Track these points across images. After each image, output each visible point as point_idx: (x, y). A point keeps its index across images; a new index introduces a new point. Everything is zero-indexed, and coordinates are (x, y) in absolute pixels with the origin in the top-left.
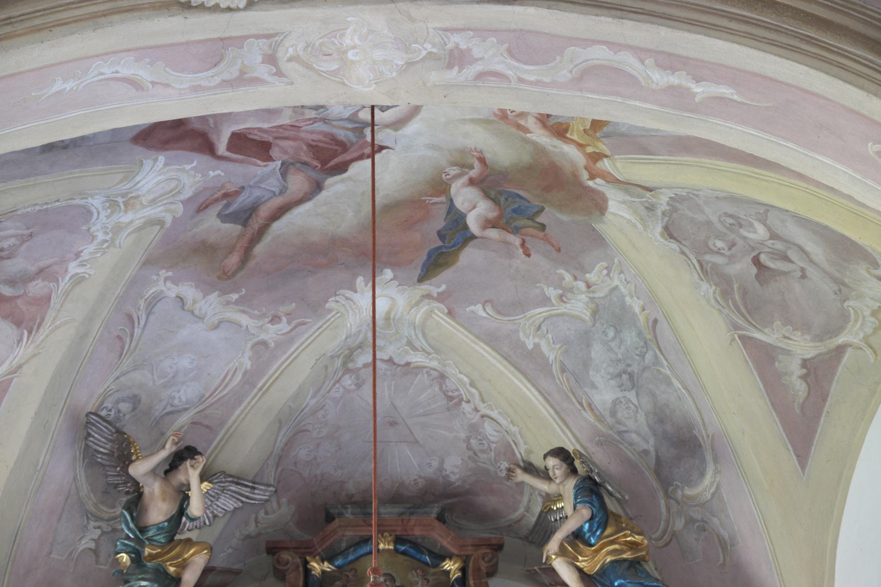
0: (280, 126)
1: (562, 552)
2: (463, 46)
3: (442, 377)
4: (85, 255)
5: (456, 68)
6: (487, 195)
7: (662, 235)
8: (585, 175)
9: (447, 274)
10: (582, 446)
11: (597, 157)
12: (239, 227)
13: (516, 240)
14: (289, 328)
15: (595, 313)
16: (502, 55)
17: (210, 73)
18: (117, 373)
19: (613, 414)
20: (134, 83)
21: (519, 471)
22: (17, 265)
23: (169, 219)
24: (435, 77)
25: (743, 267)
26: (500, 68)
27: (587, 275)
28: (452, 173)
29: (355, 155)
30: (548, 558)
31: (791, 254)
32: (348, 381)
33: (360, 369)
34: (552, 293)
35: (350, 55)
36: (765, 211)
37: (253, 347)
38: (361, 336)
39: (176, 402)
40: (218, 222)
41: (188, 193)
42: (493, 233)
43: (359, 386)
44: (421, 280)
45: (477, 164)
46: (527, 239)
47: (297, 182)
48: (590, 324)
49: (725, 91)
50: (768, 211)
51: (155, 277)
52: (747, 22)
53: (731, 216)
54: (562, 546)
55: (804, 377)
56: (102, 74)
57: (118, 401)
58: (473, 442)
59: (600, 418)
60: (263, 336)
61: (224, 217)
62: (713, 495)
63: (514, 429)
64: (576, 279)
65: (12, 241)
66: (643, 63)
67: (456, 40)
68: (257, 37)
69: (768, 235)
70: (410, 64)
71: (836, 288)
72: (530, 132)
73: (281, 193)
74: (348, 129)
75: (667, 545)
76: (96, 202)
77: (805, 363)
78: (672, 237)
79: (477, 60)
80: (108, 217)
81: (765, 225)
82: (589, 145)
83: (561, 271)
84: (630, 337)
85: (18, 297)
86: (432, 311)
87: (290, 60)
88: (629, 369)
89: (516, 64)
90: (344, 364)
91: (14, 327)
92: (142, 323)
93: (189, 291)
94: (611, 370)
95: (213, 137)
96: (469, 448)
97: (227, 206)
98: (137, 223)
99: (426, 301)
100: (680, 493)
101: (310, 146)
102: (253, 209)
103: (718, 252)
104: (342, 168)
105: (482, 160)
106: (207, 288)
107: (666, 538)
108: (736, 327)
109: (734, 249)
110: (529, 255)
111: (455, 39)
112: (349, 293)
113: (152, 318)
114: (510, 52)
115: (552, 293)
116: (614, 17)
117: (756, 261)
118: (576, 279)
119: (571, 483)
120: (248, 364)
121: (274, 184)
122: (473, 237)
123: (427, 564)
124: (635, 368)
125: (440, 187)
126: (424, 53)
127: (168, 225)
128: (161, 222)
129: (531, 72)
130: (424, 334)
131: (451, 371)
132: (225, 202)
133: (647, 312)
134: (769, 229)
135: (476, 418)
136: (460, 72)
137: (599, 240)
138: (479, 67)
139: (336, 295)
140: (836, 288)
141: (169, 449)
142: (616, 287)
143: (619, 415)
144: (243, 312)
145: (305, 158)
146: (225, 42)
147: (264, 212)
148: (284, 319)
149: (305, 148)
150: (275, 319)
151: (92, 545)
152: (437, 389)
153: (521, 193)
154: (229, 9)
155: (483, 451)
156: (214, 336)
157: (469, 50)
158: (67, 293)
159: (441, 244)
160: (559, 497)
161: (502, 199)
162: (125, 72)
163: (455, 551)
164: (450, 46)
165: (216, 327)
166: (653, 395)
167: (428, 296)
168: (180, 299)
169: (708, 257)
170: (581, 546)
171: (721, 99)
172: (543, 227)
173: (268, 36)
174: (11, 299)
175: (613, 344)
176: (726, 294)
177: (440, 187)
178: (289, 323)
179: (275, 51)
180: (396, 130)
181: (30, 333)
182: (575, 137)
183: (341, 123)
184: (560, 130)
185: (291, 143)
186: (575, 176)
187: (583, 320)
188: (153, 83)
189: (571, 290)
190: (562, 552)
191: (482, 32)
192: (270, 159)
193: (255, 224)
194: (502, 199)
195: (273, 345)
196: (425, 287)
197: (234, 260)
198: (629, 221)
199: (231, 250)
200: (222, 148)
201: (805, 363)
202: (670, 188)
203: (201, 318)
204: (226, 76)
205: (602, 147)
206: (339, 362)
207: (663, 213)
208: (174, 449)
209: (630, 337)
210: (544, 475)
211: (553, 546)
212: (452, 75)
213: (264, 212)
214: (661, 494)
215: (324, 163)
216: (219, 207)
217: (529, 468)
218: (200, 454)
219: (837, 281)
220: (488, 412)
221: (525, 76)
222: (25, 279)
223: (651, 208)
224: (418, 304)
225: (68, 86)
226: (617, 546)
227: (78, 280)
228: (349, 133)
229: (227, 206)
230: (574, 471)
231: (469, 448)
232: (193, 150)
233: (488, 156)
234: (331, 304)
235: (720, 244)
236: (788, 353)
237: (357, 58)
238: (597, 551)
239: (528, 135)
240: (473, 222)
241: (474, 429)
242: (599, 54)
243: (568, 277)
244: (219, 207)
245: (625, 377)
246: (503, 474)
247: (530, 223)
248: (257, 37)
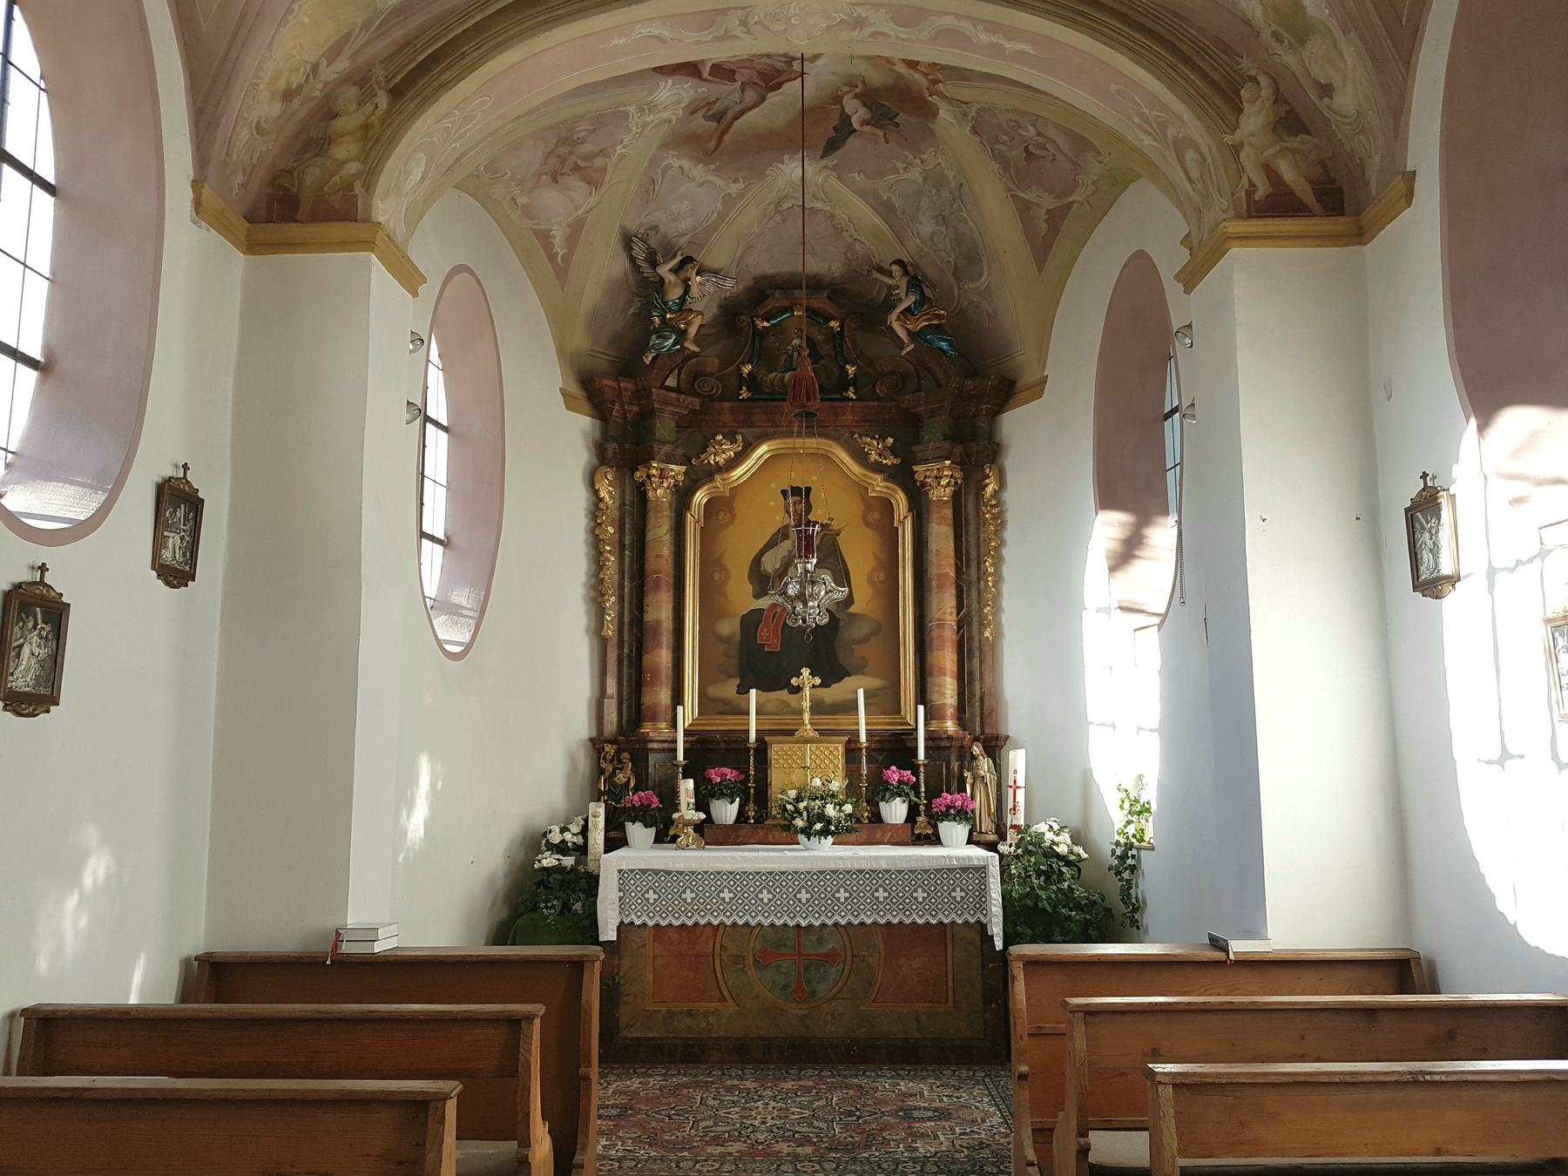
0: (741, 60)
1: (898, 319)
2: (863, 15)
3: (833, 216)
4: (626, 142)
5: (858, 30)
6: (865, 104)
7: (970, 131)
8: (927, 94)
9: (838, 153)
10: (912, 259)
11: (935, 82)
12: (715, 124)
13: (881, 133)
14: (743, 186)
15: (925, 179)
16: (887, 21)
17: (708, 31)
18: (646, 213)
19: (931, 239)
20: (659, 38)
21: (874, 271)
22: (587, 148)
23: (674, 119)
24: (844, 35)
25: (1018, 154)
26: (886, 30)
27: (923, 156)
28: (845, 90)
29: (785, 79)
30: (891, 322)
31: (1048, 146)
32: (778, 218)
33: (784, 211)
34: (900, 166)
36: (1034, 119)
37: (723, 198)
38: (786, 192)
39: (680, 230)
40: (703, 120)
41: (685, 103)
42: (867, 129)
43: (783, 221)
44: (822, 157)
45: (860, 85)
46: (888, 132)
47: (750, 95)
48: (922, 185)
49: (1026, 47)
50: (1037, 119)
51: (666, 155)
53: (1015, 121)
54: (898, 316)
55: (1046, 220)
56: (641, 33)
57: (646, 230)
58: (849, 254)
59: (923, 242)
60: (729, 191)
61: (706, 118)
62: (986, 288)
63: (873, 248)
64: (915, 158)
65: (584, 133)
66: (975, 27)
69: (1035, 133)
70: (829, 27)
71: (1073, 167)
72: (895, 65)
73: (740, 102)
74: (781, 61)
75: (957, 315)
76: (631, 109)
77: (1048, 212)
78: (976, 133)
79: (872, 24)
80: (639, 118)
81: (1034, 126)
82: (931, 74)
83: (907, 153)
84: (945, 194)
85: (588, 167)
86: (828, 176)
87: (755, 23)
88: (943, 213)
90: (776, 207)
91: (586, 185)
92: (660, 182)
93: (686, 164)
94: (932, 214)
95: (702, 68)
96: (847, 258)
97: (708, 110)
98: (656, 122)
99: (825, 170)
100: (966, 286)
101: (758, 72)
102: (723, 112)
103: (1004, 143)
104: (778, 87)
105: (864, 82)
106: (696, 161)
107: (958, 311)
108: (1010, 190)
109: (1014, 141)
110: (888, 143)
111: (860, 10)
112: (780, 165)
113: (665, 180)
114: (892, 18)
115: (900, 166)
117: (1026, 149)
118: (915, 158)
119: (905, 279)
120: (720, 207)
121: (736, 97)
122: (855, 131)
123: (820, 323)
124: (946, 213)
125: (837, 99)
126: (839, 20)
127: (674, 123)
128: (669, 121)
129: (903, 32)
130: (823, 191)
131: (838, 213)
132: (707, 108)
133: (956, 179)
134: (1037, 130)
135: (851, 240)
137: (932, 135)
138: (873, 29)
139: (771, 166)
140: (1073, 167)
141: (679, 258)
142: (940, 163)
143: (935, 239)
144: (717, 176)
145: (755, 81)
147: (730, 114)
148: (741, 180)
149: (755, 73)
150: (736, 181)
151: (637, 311)
152: (829, 223)
153: (886, 103)
155: (854, 260)
156: (700, 190)
157: (867, 17)
158: (616, 165)
159: (835, 135)
160: (898, 287)
161: (874, 107)
162: (656, 32)
163: (836, 315)
164: (855, 15)
165: (702, 185)
166: (956, 229)
167: (826, 167)
168: (681, 168)
169: (997, 146)
170: (909, 316)
171: (1023, 52)
172: (898, 125)
173: (743, 8)
174: (584, 168)
175: (934, 198)
176: (1006, 168)
177: (837, 99)
178: (744, 182)
179: (746, 18)
180: (812, 62)
181: (596, 188)
182: (923, 69)
183: (780, 58)
184: (913, 65)
185: (747, 71)
186: (921, 93)
187: (917, 184)
189: (911, 164)
190: (898, 319)
192: (735, 81)
193: (725, 122)
194: (874, 107)
195: (734, 196)
196: (825, 162)
197: (711, 145)
198: (951, 122)
199: (711, 138)
200: (706, 75)
201: (1048, 212)
202: (978, 103)
203: (694, 180)
204: (716, 34)
205: (940, 76)
206: (772, 206)
207: (972, 117)
208: (681, 258)
209: (945, 194)
210: (890, 274)
211: (893, 317)
213: (730, 114)
214: (956, 286)
215: (766, 84)
216: (703, 111)
217: (880, 270)
218: (695, 261)
219: (1074, 163)
220: (859, 238)
222: (592, 156)
223: (965, 115)
224: (820, 171)
225: (621, 41)
226: (929, 316)
227: (622, 157)
228: (783, 65)
229: (708, 110)
230: (906, 273)
231: (847, 258)
232: (688, 75)
233: (867, 80)
234: (768, 172)
235: (1005, 138)
236: (1039, 206)
237: (796, 23)
238: (918, 319)
239: (894, 67)
240: (856, 124)
241: (850, 247)
243: (911, 157)
244: (703, 111)
245: (940, 217)
246: (866, 273)
247: (889, 122)
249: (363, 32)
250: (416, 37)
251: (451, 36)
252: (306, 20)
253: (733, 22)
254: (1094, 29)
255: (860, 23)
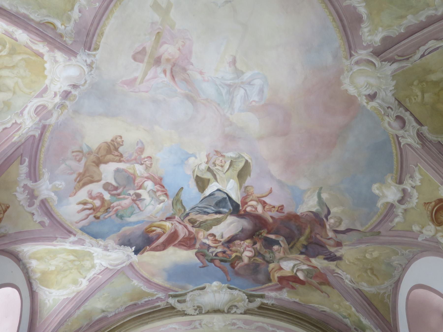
2: (235, 322)
5: (233, 326)
24: (230, 328)
26: (241, 326)
35: (214, 324)
52: (289, 319)
66: (268, 326)
67: (234, 321)
68: (198, 320)
70: (225, 325)
87: (204, 324)
89: (244, 325)
116: (263, 317)
126: (228, 323)
136: (234, 326)
138: (238, 326)
146: (192, 321)
154: (194, 315)
162: (174, 327)
164: (233, 322)
173: (201, 320)
188: (178, 329)
191: (239, 320)
204: (192, 327)
212: (233, 327)
221: (246, 328)
242: (260, 324)
248: (198, 320)
249: (86, 327)
250: (102, 328)
251: (112, 328)
252: (70, 324)
253: (197, 324)
254: (302, 327)
255: (234, 324)
